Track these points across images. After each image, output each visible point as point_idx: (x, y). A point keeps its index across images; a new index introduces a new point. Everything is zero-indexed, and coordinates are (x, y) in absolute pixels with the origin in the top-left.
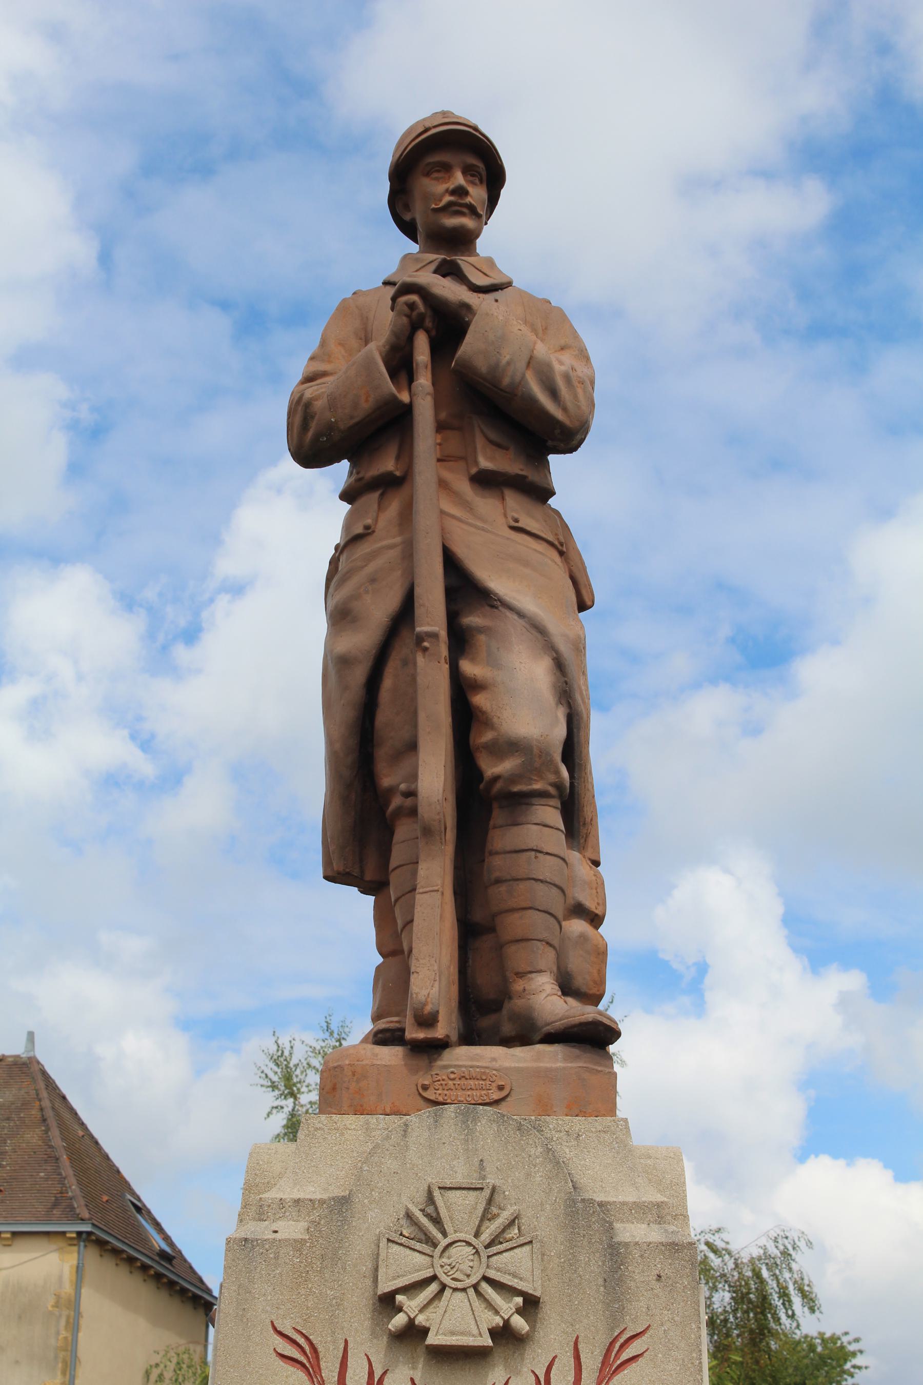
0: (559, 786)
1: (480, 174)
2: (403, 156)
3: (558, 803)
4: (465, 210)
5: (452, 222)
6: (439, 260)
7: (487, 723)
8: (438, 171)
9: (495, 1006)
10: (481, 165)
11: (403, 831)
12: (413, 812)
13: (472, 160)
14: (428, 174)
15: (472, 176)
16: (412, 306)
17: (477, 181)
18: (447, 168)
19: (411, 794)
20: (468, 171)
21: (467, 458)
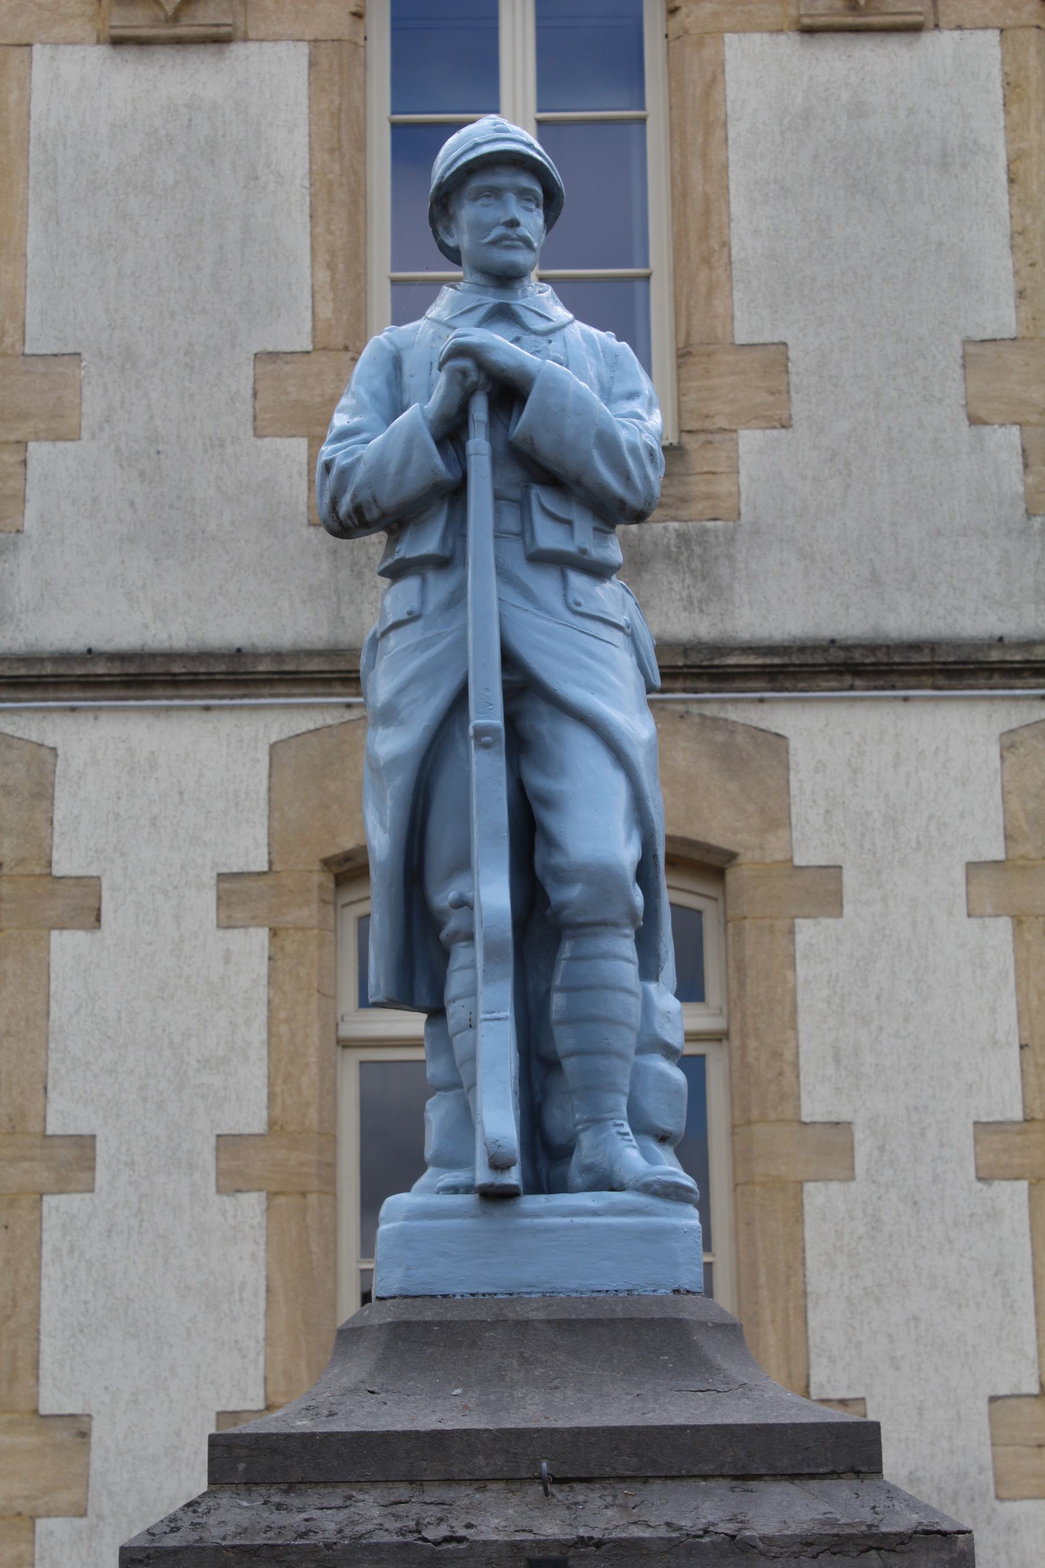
0: (633, 917)
1: (536, 199)
2: (537, 1221)
3: (630, 931)
4: (520, 243)
5: (503, 257)
6: (491, 305)
7: (552, 843)
8: (488, 196)
9: (563, 1152)
10: (539, 191)
11: (460, 955)
12: (470, 937)
13: (526, 182)
14: (475, 199)
15: (529, 200)
16: (464, 373)
17: (533, 206)
18: (496, 193)
19: (464, 904)
20: (524, 194)
21: (525, 532)
